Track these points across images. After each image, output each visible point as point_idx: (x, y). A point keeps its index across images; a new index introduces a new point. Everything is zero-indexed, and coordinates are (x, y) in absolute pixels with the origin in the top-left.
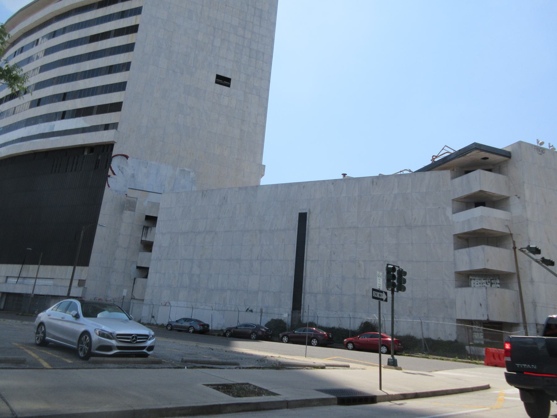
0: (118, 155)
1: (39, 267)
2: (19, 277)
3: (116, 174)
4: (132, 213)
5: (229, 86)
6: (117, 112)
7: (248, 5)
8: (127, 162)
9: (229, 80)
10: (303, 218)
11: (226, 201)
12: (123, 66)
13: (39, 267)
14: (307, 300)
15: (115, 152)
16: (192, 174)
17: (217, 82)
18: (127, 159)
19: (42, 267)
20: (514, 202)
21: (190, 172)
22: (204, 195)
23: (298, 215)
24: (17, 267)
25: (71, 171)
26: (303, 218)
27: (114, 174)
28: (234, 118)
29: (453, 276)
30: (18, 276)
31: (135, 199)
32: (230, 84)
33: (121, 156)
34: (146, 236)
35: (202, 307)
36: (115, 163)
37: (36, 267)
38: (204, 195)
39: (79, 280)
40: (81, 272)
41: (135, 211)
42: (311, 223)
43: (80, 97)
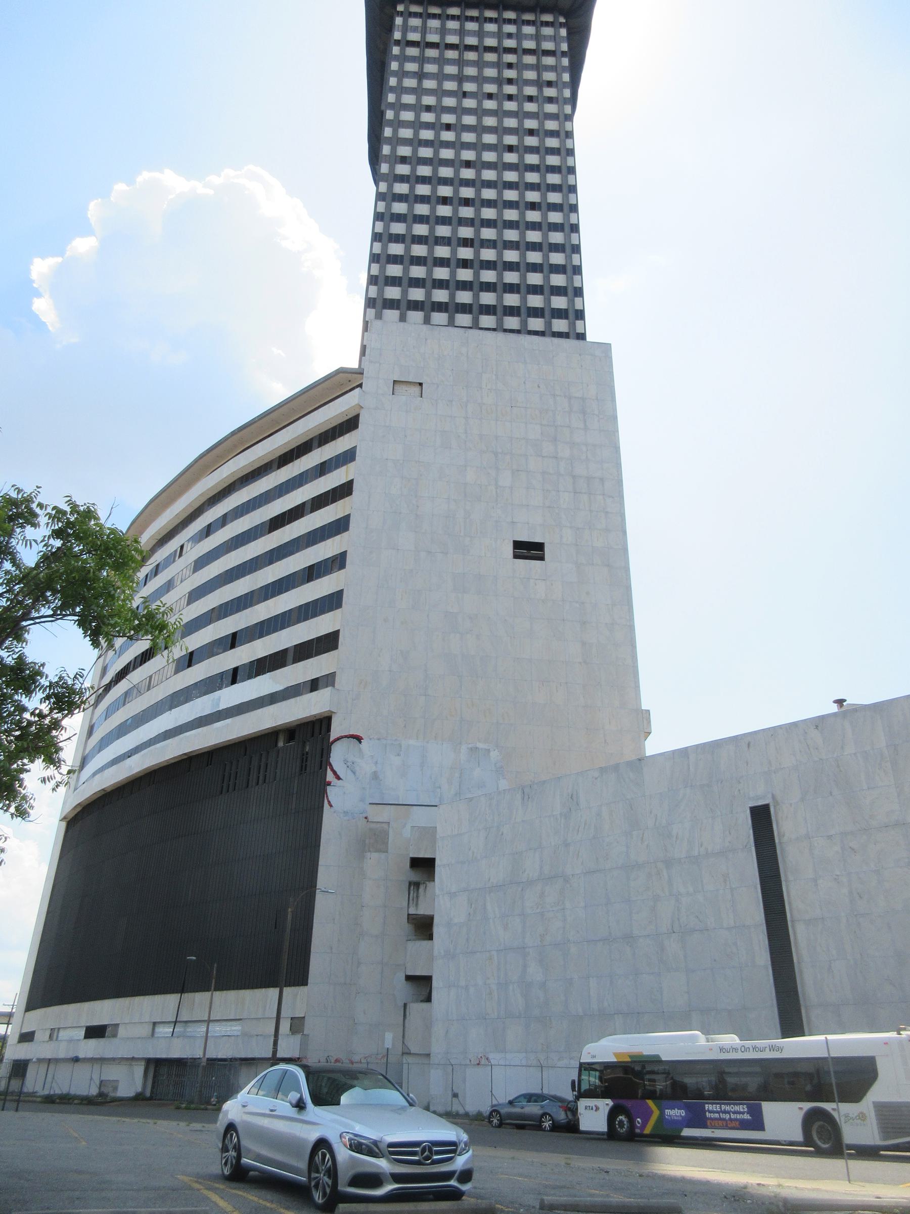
0: (342, 737)
1: (212, 995)
2: (175, 1022)
3: (341, 777)
4: (383, 855)
5: (542, 558)
7: (554, 395)
8: (360, 750)
9: (540, 547)
13: (212, 995)
16: (494, 755)
17: (516, 556)
18: (360, 742)
22: (526, 797)
23: (748, 811)
24: (171, 1000)
25: (258, 784)
27: (338, 778)
28: (564, 620)
30: (174, 1020)
31: (385, 826)
32: (544, 554)
33: (348, 738)
34: (417, 905)
36: (338, 755)
37: (207, 995)
38: (526, 797)
39: (292, 1018)
41: (387, 852)
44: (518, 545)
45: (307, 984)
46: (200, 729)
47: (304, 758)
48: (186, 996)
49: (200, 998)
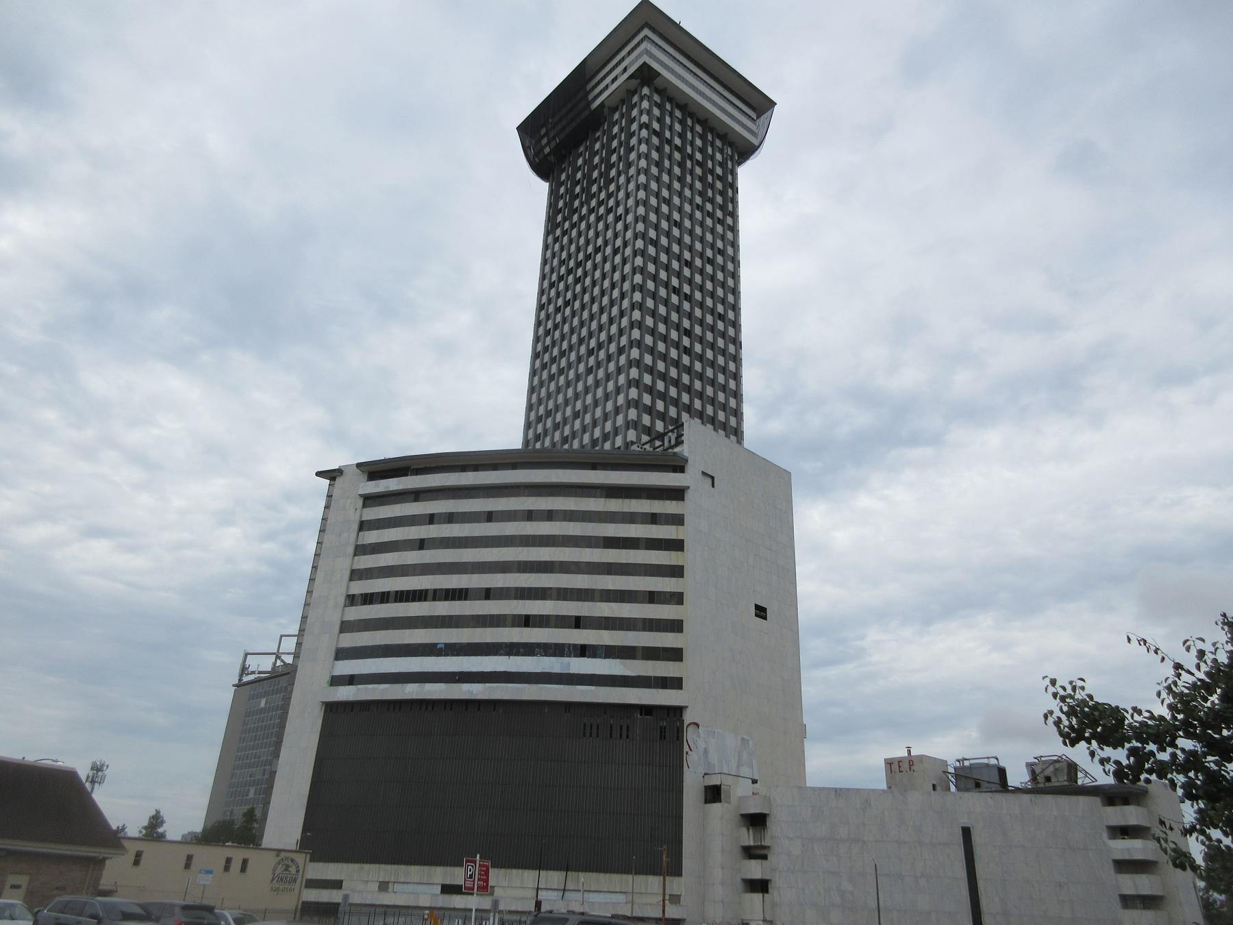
2: (564, 890)
5: (765, 618)
6: (677, 663)
8: (699, 733)
10: (966, 832)
11: (870, 804)
12: (671, 596)
15: (688, 717)
17: (756, 615)
19: (640, 879)
26: (966, 832)
27: (691, 750)
29: (1118, 898)
30: (563, 888)
36: (690, 735)
37: (630, 877)
40: (676, 885)
41: (730, 803)
42: (976, 839)
44: (758, 607)
45: (681, 875)
47: (663, 730)
48: (569, 873)
49: (583, 876)
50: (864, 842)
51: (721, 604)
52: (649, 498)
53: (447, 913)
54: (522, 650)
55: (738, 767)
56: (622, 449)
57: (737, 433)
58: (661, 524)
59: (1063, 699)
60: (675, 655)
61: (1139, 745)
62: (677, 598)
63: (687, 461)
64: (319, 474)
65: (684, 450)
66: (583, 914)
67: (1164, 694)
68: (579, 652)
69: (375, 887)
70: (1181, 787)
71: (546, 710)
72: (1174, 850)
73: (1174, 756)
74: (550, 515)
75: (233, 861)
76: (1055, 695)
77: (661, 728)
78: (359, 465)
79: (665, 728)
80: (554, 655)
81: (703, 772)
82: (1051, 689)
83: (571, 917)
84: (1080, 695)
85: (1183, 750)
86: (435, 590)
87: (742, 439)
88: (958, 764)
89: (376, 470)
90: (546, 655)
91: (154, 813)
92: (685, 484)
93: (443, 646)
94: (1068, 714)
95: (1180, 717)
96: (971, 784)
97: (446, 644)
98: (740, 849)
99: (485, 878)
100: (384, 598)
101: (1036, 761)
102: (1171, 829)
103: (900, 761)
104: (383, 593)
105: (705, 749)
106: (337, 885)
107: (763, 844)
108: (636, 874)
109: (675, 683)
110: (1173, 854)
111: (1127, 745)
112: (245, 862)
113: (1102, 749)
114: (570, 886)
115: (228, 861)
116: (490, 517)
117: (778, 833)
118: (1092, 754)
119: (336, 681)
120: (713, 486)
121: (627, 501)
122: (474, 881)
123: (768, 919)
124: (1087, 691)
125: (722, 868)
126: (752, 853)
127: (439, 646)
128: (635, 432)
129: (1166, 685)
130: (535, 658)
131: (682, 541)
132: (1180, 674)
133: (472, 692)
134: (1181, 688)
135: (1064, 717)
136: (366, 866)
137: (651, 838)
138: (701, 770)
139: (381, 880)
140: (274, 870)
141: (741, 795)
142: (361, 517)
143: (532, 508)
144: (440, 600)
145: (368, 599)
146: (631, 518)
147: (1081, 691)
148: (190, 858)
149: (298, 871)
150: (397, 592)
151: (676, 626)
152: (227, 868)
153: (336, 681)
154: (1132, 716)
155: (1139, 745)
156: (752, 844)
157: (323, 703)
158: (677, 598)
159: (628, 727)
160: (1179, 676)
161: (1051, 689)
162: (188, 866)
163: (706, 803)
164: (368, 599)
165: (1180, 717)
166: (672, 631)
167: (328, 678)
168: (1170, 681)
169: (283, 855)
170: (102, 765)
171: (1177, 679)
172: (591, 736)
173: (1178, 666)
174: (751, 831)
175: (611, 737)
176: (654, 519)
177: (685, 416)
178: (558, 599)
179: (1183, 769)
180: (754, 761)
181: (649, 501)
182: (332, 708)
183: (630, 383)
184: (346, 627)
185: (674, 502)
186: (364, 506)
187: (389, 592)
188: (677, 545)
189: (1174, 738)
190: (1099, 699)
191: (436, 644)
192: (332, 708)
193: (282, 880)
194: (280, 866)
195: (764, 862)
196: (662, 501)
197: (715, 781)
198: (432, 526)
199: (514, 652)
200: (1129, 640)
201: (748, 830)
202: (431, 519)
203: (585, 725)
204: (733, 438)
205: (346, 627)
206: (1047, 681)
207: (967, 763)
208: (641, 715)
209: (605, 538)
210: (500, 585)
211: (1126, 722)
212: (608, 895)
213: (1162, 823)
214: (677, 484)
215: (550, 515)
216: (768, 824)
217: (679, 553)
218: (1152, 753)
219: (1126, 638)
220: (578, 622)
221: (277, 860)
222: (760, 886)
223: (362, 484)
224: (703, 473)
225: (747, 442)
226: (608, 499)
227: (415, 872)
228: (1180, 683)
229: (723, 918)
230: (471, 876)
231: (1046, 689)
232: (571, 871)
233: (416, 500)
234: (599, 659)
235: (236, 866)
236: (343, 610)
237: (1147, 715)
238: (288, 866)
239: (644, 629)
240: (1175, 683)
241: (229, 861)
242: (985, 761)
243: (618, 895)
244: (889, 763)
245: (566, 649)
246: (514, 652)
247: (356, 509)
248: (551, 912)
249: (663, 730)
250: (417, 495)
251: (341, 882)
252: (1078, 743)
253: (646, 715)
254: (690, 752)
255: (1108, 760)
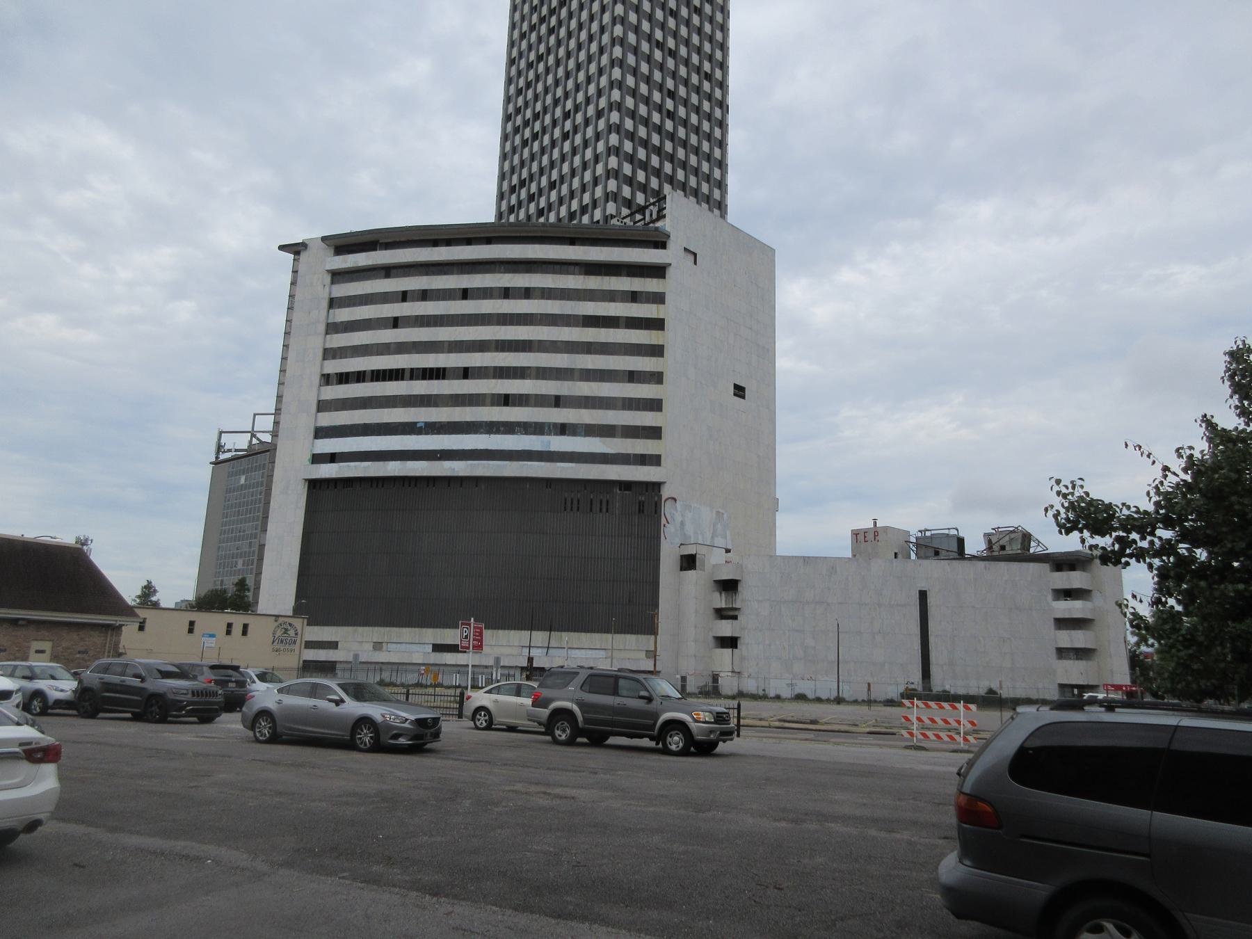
0: (669, 498)
2: (548, 648)
5: (743, 397)
7: (752, 282)
10: (923, 595)
11: (836, 572)
12: (651, 375)
14: (934, 670)
15: (666, 492)
17: (735, 395)
19: (619, 638)
20: (1096, 594)
21: (723, 514)
24: (526, 633)
25: (601, 510)
26: (923, 595)
27: (668, 523)
29: (1055, 651)
35: (823, 679)
36: (667, 509)
37: (610, 636)
41: (704, 570)
42: (931, 601)
43: (586, 407)
46: (543, 464)
47: (641, 504)
48: (552, 633)
49: (566, 636)
50: (828, 604)
51: (701, 383)
52: (629, 275)
53: (441, 668)
54: (502, 429)
55: (712, 537)
56: (601, 222)
57: (721, 206)
58: (641, 303)
59: (1065, 496)
60: (654, 433)
61: (1125, 534)
62: (657, 378)
63: (669, 236)
64: (282, 248)
65: (666, 225)
66: (592, 668)
67: (1152, 494)
68: (559, 431)
69: (370, 647)
70: (1156, 569)
71: (528, 486)
72: (1132, 614)
73: (1152, 543)
74: (527, 293)
75: (234, 626)
76: (1059, 493)
77: (640, 502)
78: (324, 239)
79: (643, 502)
80: (535, 433)
81: (680, 543)
82: (1056, 488)
83: (580, 671)
84: (1079, 492)
85: (1160, 538)
86: (412, 370)
87: (726, 212)
88: (920, 534)
89: (343, 244)
90: (526, 434)
91: (146, 583)
92: (667, 261)
93: (423, 425)
94: (1067, 509)
95: (1162, 512)
96: (931, 552)
97: (426, 423)
98: (712, 610)
99: (479, 638)
100: (360, 377)
101: (994, 531)
102: (1141, 601)
103: (866, 532)
104: (359, 373)
105: (682, 521)
106: (333, 645)
107: (734, 606)
108: (615, 633)
109: (655, 460)
110: (1131, 617)
111: (1114, 534)
112: (245, 627)
113: (1093, 537)
114: (553, 644)
115: (230, 625)
116: (465, 294)
117: (747, 597)
118: (1083, 541)
119: (317, 459)
120: (695, 263)
121: (606, 278)
122: (469, 641)
123: (736, 670)
124: (1084, 490)
125: (696, 627)
126: (721, 614)
127: (418, 425)
128: (615, 205)
129: (1154, 485)
130: (515, 436)
131: (662, 321)
132: (1167, 476)
133: (454, 469)
134: (1166, 487)
135: (1062, 511)
136: (360, 629)
137: (629, 601)
138: (678, 541)
139: (375, 641)
140: (274, 633)
141: (715, 563)
142: (330, 294)
143: (508, 286)
144: (417, 379)
145: (344, 378)
146: (611, 296)
147: (1080, 489)
148: (192, 624)
149: (296, 634)
150: (373, 371)
151: (655, 405)
152: (228, 632)
153: (317, 459)
154: (1121, 510)
155: (1125, 534)
156: (724, 606)
157: (306, 480)
158: (657, 378)
159: (607, 502)
160: (1165, 477)
161: (1056, 488)
162: (191, 631)
163: (681, 570)
164: (344, 378)
165: (1162, 512)
166: (652, 409)
167: (309, 456)
168: (1157, 482)
169: (281, 620)
170: (87, 540)
171: (1163, 480)
172: (572, 510)
173: (1166, 469)
174: (723, 595)
175: (591, 510)
176: (634, 297)
177: (667, 188)
178: (537, 378)
179: (1157, 554)
180: (728, 533)
181: (629, 278)
182: (315, 485)
183: (609, 151)
184: (323, 406)
185: (655, 280)
186: (333, 283)
187: (365, 372)
188: (657, 324)
189: (1154, 529)
190: (1094, 495)
191: (415, 423)
192: (315, 485)
193: (282, 642)
194: (279, 630)
195: (734, 621)
196: (643, 279)
197: (690, 550)
198: (405, 304)
199: (494, 430)
200: (1126, 445)
201: (721, 594)
202: (404, 296)
203: (566, 500)
204: (717, 212)
205: (323, 406)
206: (1053, 480)
207: (928, 534)
208: (620, 490)
209: (583, 316)
210: (478, 365)
211: (1117, 515)
212: (590, 652)
213: (1134, 596)
214: (657, 262)
215: (527, 293)
216: (739, 589)
217: (660, 332)
218: (1134, 541)
219: (1124, 444)
220: (557, 401)
221: (277, 624)
222: (730, 642)
223: (329, 259)
224: (686, 249)
225: (731, 217)
226: (586, 277)
227: (407, 633)
228: (1166, 483)
229: (695, 670)
230: (466, 637)
231: (1052, 488)
232: (555, 631)
233: (387, 276)
234: (579, 438)
235: (237, 629)
236: (319, 389)
237: (1134, 509)
238: (286, 630)
239: (624, 408)
240: (1162, 483)
241: (230, 625)
242: (946, 532)
243: (597, 651)
244: (855, 534)
245: (546, 428)
246: (494, 430)
247: (324, 286)
248: (562, 667)
249: (641, 504)
250: (388, 271)
251: (337, 642)
252: (1071, 532)
253: (625, 490)
254: (667, 524)
255: (1096, 546)
